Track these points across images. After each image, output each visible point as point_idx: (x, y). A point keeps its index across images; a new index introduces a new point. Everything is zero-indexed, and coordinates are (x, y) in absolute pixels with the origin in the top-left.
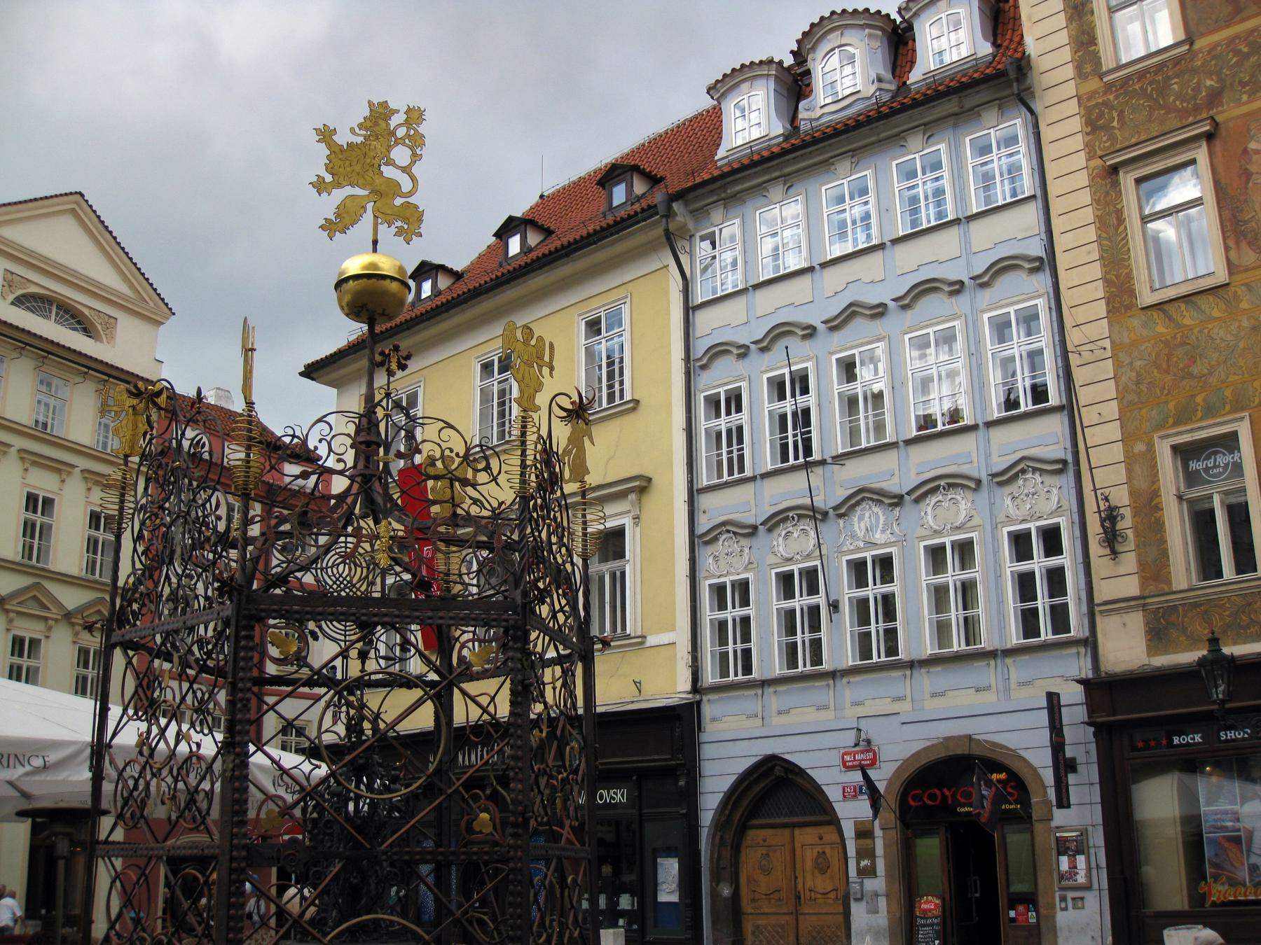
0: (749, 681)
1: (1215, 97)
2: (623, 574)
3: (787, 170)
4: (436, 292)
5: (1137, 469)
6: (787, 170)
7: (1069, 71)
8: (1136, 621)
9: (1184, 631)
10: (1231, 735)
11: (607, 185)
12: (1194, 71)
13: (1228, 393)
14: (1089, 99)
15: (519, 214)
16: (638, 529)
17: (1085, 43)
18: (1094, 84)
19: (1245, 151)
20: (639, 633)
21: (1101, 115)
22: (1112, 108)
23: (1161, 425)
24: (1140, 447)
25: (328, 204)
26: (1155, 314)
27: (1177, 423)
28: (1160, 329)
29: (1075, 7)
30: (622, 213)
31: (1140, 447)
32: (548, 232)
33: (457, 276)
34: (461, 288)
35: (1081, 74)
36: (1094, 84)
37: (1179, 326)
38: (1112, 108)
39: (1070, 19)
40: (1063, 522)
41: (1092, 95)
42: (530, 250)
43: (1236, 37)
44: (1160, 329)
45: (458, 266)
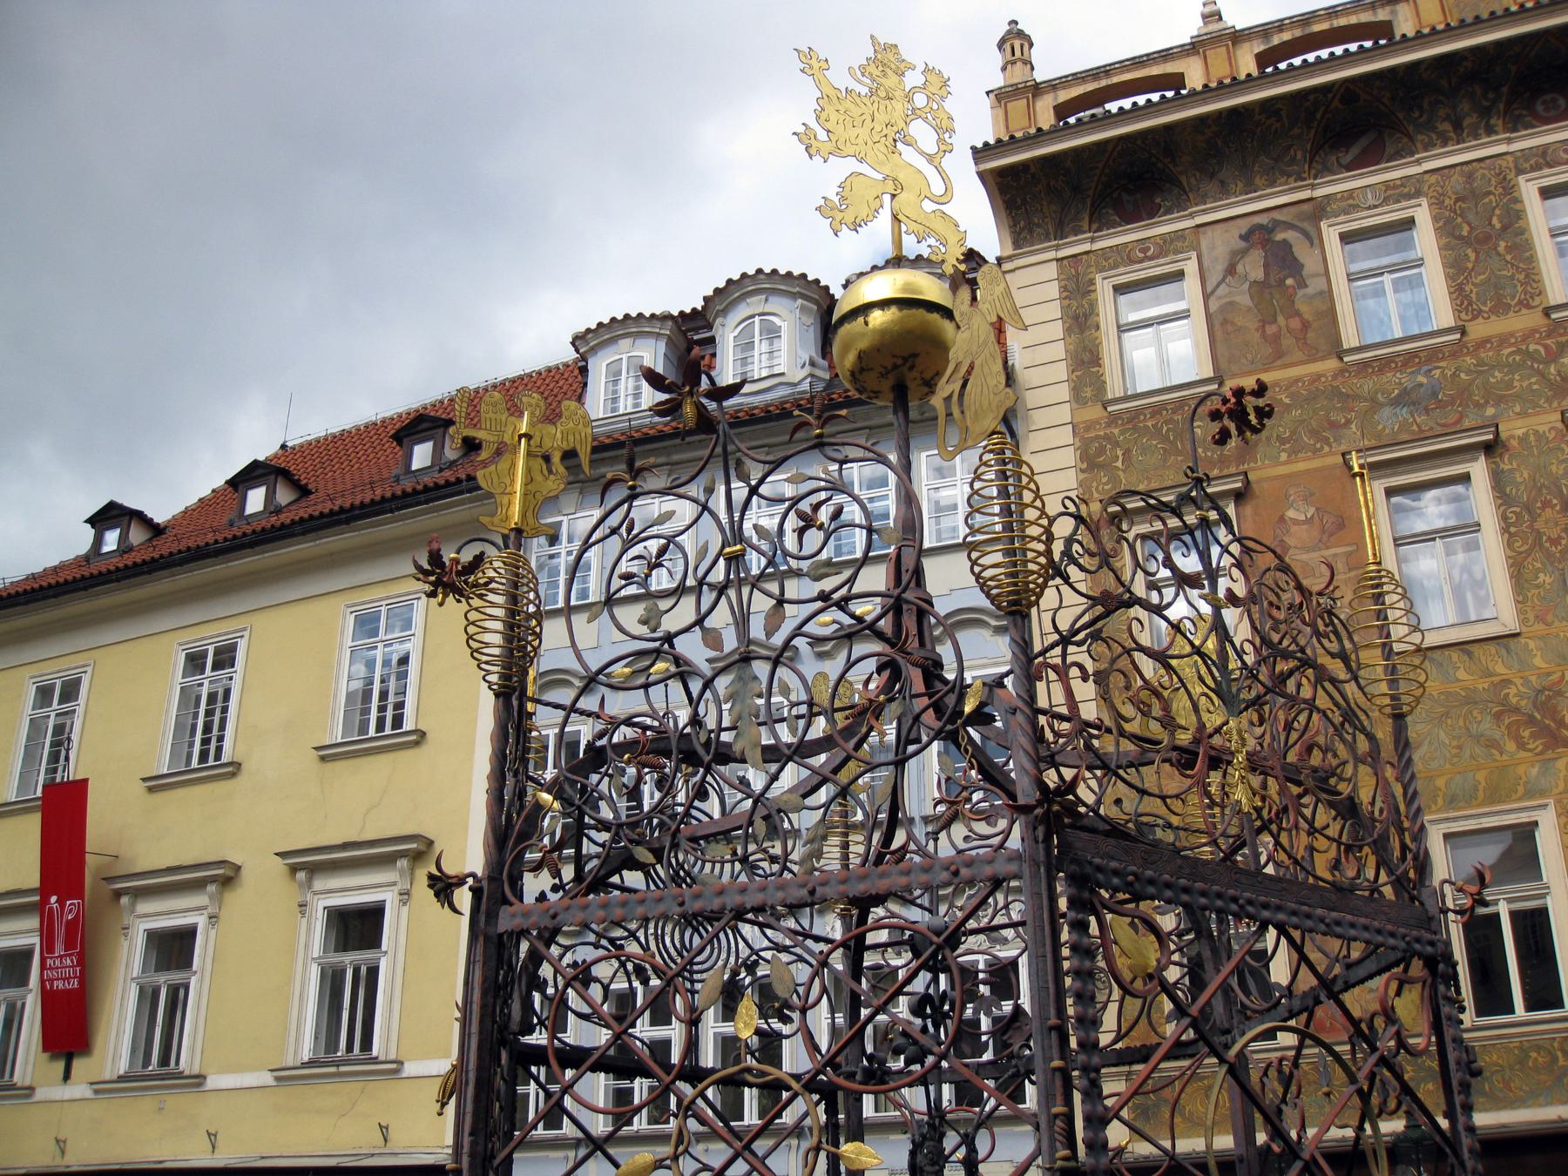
0: (556, 1139)
2: (373, 972)
3: (676, 457)
4: (124, 548)
6: (676, 457)
7: (1064, 392)
11: (405, 441)
14: (1087, 429)
15: (261, 458)
16: (405, 909)
17: (1086, 362)
18: (1095, 412)
19: (1282, 519)
20: (392, 1057)
21: (1101, 451)
22: (1117, 444)
25: (831, 175)
29: (1076, 318)
30: (427, 480)
32: (304, 491)
33: (156, 530)
34: (165, 546)
35: (1077, 397)
36: (1095, 412)
38: (1117, 444)
39: (1068, 331)
41: (1090, 426)
42: (279, 511)
45: (160, 516)
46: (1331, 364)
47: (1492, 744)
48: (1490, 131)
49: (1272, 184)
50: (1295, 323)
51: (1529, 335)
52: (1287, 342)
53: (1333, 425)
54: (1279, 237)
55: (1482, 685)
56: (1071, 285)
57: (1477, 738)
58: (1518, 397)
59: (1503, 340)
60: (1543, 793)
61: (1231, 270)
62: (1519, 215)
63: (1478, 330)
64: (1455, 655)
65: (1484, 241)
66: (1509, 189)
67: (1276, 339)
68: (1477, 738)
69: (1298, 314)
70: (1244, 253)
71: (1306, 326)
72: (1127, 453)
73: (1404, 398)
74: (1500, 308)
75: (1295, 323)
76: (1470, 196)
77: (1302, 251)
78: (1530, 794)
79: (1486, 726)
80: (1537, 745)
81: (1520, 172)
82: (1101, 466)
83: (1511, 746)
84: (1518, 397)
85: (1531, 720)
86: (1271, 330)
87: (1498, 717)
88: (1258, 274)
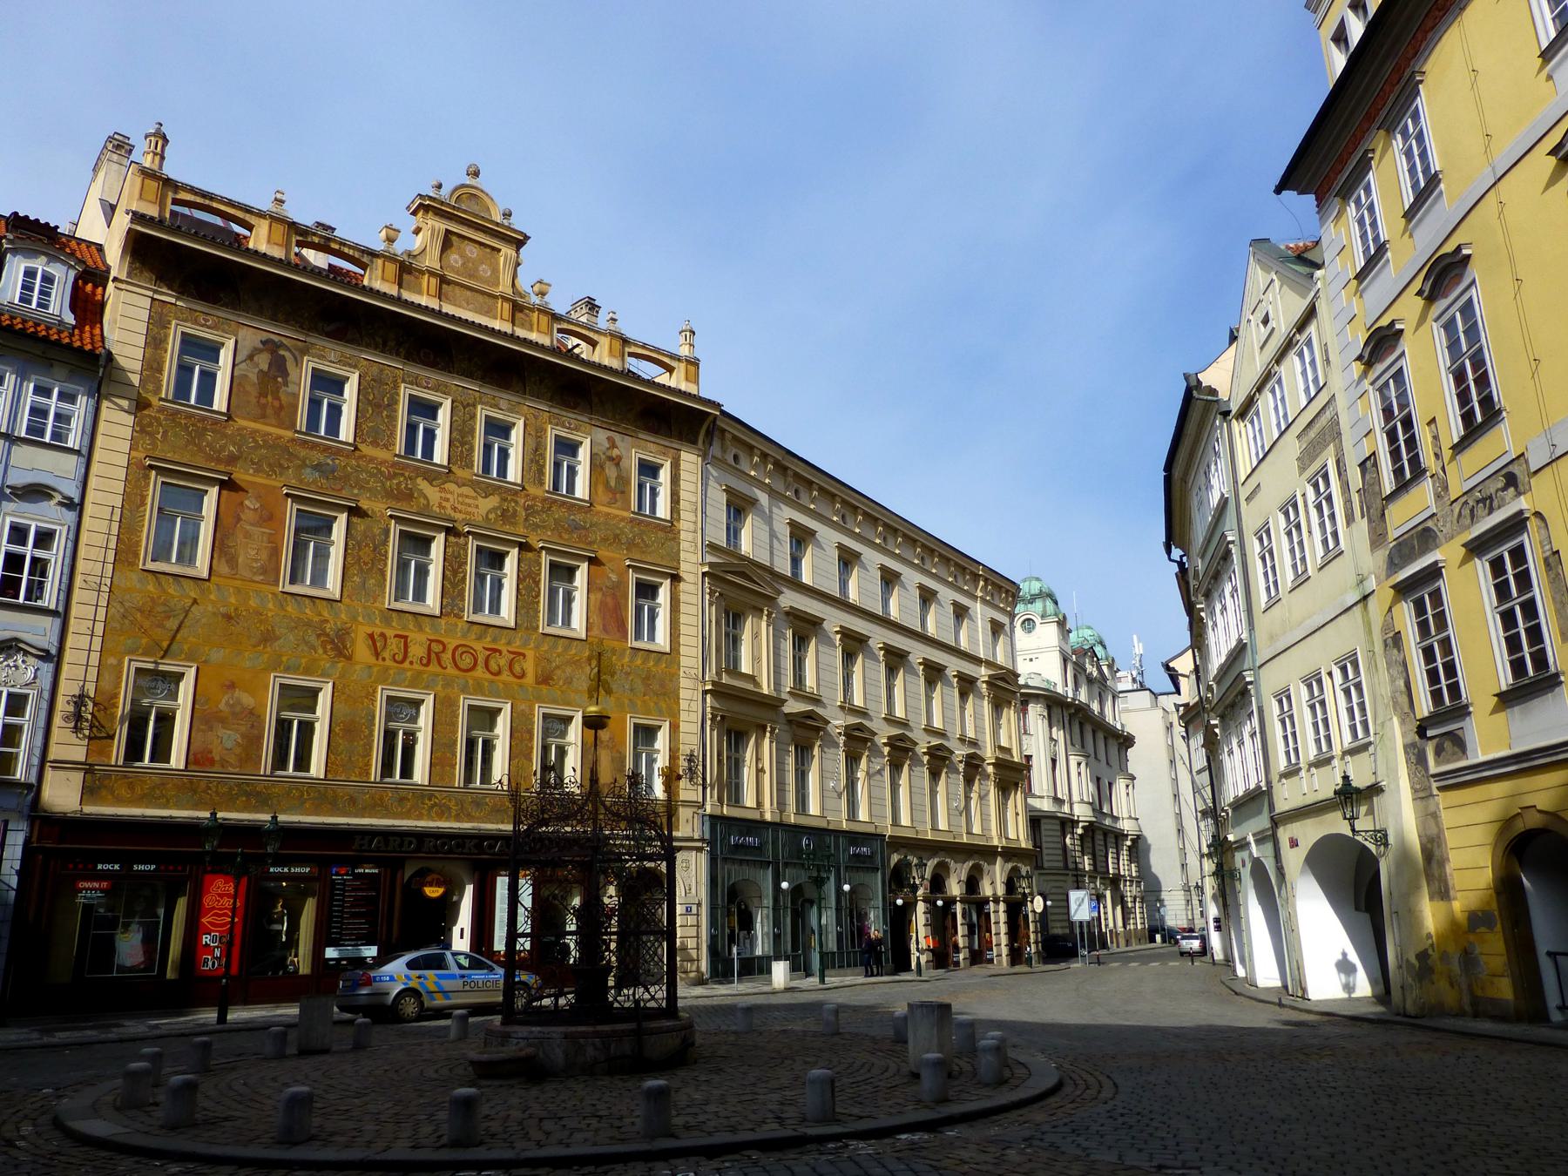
1: (232, 460)
5: (106, 675)
8: (77, 778)
9: (112, 793)
10: (141, 867)
12: (225, 436)
13: (186, 647)
21: (151, 425)
23: (132, 652)
24: (112, 661)
26: (150, 576)
27: (143, 654)
28: (151, 588)
29: (154, 339)
31: (112, 661)
37: (164, 591)
40: (32, 693)
43: (257, 431)
44: (151, 588)
46: (289, 434)
47: (313, 648)
48: (398, 354)
49: (286, 322)
50: (276, 404)
51: (383, 462)
52: (269, 411)
53: (281, 466)
54: (282, 352)
55: (316, 619)
56: (156, 317)
57: (307, 643)
58: (369, 490)
59: (372, 459)
60: (329, 676)
61: (251, 357)
62: (397, 402)
63: (366, 449)
64: (307, 601)
65: (378, 406)
66: (396, 387)
67: (264, 407)
68: (307, 643)
69: (278, 399)
70: (260, 351)
71: (281, 407)
72: (165, 433)
73: (318, 467)
74: (375, 444)
75: (276, 404)
76: (378, 381)
77: (290, 365)
78: (322, 675)
79: (313, 639)
80: (332, 654)
81: (404, 381)
82: (148, 433)
83: (320, 651)
84: (369, 490)
85: (332, 642)
86: (263, 401)
87: (319, 636)
88: (265, 367)
